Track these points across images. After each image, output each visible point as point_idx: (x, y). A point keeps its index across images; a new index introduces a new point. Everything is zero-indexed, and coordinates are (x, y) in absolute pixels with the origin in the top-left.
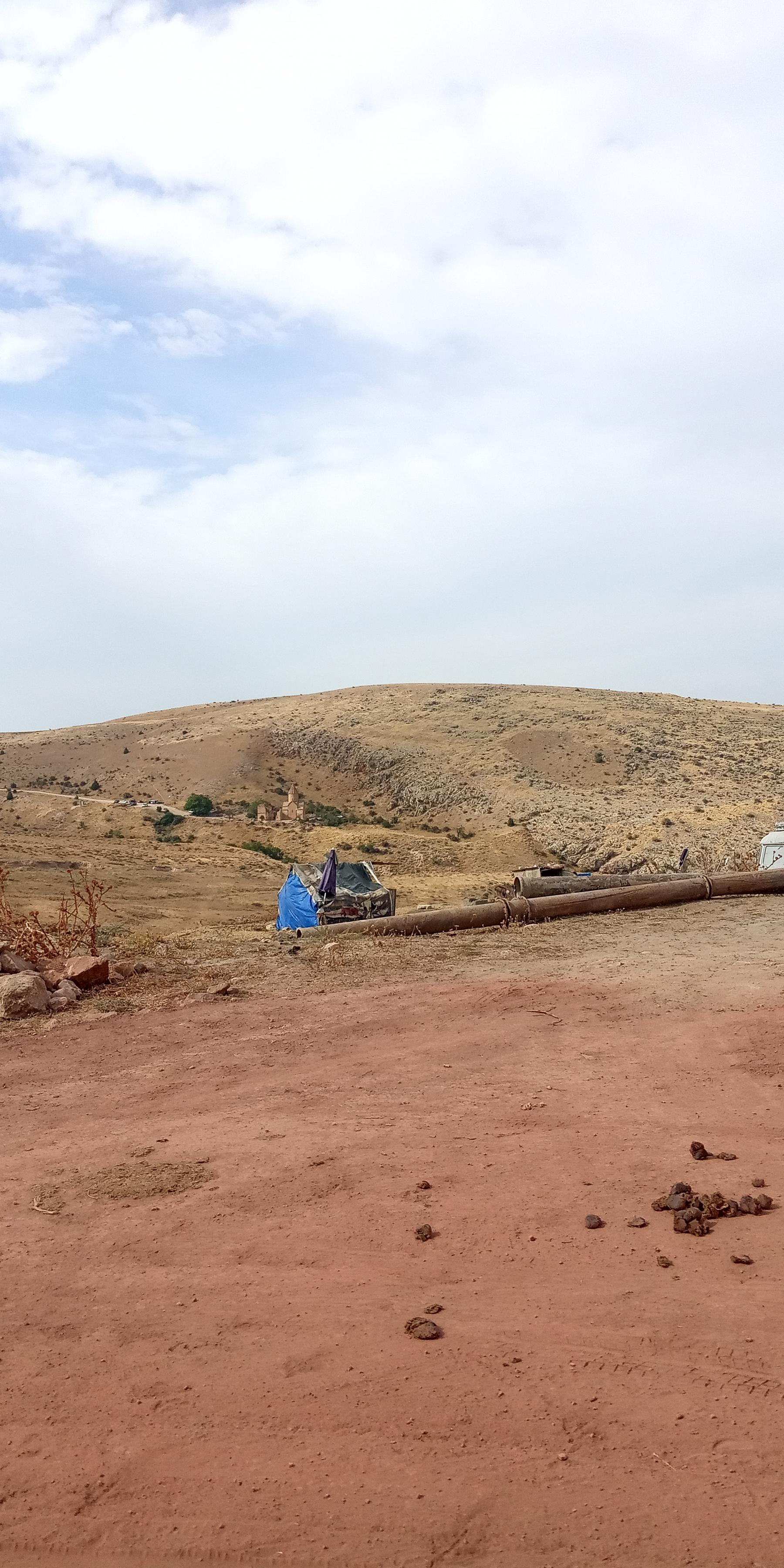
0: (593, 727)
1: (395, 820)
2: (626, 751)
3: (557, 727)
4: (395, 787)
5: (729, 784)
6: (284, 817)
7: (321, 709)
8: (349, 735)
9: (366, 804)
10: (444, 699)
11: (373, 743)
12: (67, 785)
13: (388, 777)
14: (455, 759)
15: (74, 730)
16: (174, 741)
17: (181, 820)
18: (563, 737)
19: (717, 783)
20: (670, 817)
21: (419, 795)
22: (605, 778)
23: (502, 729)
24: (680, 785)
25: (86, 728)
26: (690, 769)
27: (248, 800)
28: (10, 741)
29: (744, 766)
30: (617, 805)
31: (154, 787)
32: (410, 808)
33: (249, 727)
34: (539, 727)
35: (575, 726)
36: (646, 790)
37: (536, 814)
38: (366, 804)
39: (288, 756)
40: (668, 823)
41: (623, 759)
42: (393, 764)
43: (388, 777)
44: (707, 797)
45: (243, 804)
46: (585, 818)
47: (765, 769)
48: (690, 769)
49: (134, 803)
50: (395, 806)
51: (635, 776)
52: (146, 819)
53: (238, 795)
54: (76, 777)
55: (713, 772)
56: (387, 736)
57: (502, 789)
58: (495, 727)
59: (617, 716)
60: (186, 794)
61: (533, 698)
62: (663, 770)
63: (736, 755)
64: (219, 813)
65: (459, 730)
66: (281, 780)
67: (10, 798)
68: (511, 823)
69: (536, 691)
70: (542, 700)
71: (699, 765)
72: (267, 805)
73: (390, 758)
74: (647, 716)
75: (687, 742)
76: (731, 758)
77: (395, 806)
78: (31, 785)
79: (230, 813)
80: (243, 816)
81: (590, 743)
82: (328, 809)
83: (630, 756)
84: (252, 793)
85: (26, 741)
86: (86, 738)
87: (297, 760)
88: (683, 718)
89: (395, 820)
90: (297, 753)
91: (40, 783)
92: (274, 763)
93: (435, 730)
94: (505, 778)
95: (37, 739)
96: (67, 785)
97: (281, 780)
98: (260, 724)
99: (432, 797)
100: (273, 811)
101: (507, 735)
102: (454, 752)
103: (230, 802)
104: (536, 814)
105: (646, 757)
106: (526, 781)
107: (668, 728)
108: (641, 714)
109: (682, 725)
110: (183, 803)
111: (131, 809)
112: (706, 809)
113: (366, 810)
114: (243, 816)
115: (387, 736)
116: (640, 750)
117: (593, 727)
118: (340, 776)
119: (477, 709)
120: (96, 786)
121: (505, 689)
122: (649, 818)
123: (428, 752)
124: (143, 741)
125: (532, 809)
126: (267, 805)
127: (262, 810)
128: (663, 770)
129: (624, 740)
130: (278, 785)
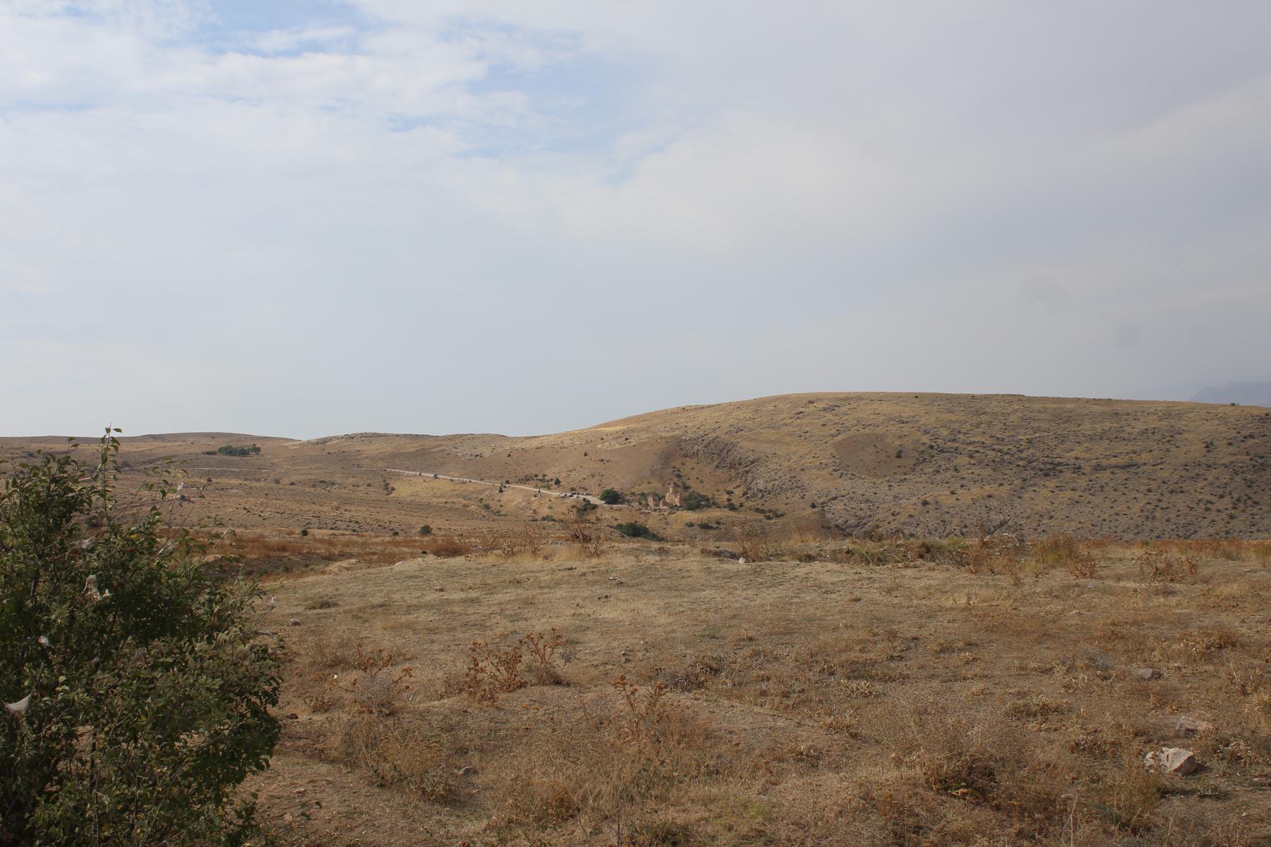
1: (741, 505)
3: (879, 431)
4: (750, 479)
11: (745, 448)
24: (948, 475)
35: (894, 429)
36: (924, 478)
41: (916, 454)
42: (752, 463)
44: (964, 482)
51: (918, 469)
56: (756, 440)
58: (834, 431)
73: (751, 459)
81: (897, 443)
89: (741, 505)
93: (791, 435)
101: (839, 438)
112: (960, 491)
115: (756, 440)
116: (931, 447)
117: (906, 429)
119: (829, 416)
129: (925, 439)
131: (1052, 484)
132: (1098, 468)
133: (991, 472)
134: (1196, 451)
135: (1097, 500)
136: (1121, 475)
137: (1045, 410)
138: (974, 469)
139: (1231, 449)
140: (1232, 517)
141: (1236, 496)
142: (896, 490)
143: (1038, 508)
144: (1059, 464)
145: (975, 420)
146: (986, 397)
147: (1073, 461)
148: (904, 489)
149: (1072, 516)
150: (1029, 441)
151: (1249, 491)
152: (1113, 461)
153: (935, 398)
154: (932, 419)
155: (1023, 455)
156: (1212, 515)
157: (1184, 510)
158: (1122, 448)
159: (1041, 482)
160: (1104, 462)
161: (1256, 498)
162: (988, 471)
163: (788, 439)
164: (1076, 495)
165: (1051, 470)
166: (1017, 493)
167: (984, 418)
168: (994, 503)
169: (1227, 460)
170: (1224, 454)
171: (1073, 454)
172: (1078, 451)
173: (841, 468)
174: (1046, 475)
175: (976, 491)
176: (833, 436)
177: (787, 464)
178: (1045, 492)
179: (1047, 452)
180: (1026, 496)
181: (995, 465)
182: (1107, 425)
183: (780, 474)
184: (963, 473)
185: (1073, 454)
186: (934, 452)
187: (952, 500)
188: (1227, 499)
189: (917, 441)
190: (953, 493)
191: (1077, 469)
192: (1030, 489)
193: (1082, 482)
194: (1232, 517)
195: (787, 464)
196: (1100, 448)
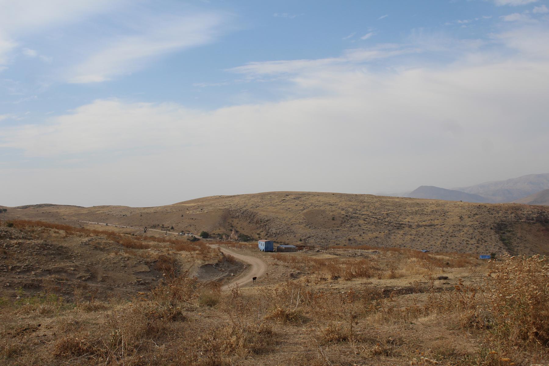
0: (334, 208)
2: (343, 216)
3: (321, 208)
5: (373, 227)
6: (231, 239)
7: (247, 201)
8: (255, 211)
9: (258, 234)
10: (288, 198)
11: (262, 214)
12: (163, 227)
13: (266, 225)
14: (287, 219)
15: (165, 207)
16: (198, 213)
17: (198, 240)
18: (324, 211)
19: (369, 227)
20: (351, 238)
21: (274, 231)
22: (334, 225)
23: (304, 209)
24: (357, 228)
25: (169, 206)
26: (361, 222)
27: (220, 233)
28: (143, 211)
29: (379, 221)
30: (335, 234)
31: (191, 229)
32: (271, 235)
33: (223, 208)
34: (316, 208)
35: (328, 208)
36: (346, 229)
37: (309, 237)
38: (258, 234)
39: (235, 218)
40: (350, 240)
41: (341, 219)
42: (267, 221)
43: (266, 225)
44: (364, 231)
45: (219, 234)
46: (324, 239)
47: (386, 222)
48: (361, 222)
49: (184, 234)
50: (267, 235)
51: (343, 225)
52: (188, 239)
53: (217, 231)
54: (166, 225)
55: (369, 223)
56: (267, 211)
57: (301, 229)
58: (302, 208)
59: (343, 204)
60: (201, 231)
61: (317, 197)
62: (353, 223)
63: (378, 217)
64: (211, 237)
65: (290, 209)
66: (232, 226)
67: (145, 232)
68: (301, 240)
69: (319, 194)
70: (320, 198)
71: (365, 220)
72: (226, 234)
73: (266, 219)
74: (353, 204)
75: (363, 213)
76: (376, 218)
77: (267, 235)
78: (151, 227)
79: (214, 238)
80: (218, 238)
81: (331, 214)
82: (246, 236)
83: (343, 218)
84: (222, 230)
85: (149, 211)
86: (169, 210)
87: (238, 219)
88: (365, 204)
90: (238, 217)
91: (154, 227)
92: (230, 221)
94: (302, 226)
95: (152, 211)
96: (163, 227)
97: (232, 226)
98: (226, 207)
99: (278, 232)
100: (228, 236)
101: (305, 211)
102: (287, 217)
103: (214, 234)
104: (309, 237)
105: (348, 218)
106: (308, 227)
107: (359, 208)
108: (351, 203)
109: (364, 207)
110: (200, 234)
111: (184, 236)
112: (363, 235)
113: (258, 236)
114: (218, 238)
115: (267, 211)
116: (347, 216)
118: (251, 225)
120: (172, 228)
121: (309, 194)
122: (345, 238)
123: (279, 217)
124: (188, 212)
125: (309, 236)
126: (226, 234)
127: (224, 237)
128: (353, 223)
129: (343, 212)
130: (231, 228)
131: (401, 232)
132: (418, 226)
133: (374, 227)
134: (456, 220)
135: (422, 239)
136: (429, 229)
137: (389, 202)
138: (367, 226)
139: (470, 219)
140: (478, 247)
141: (477, 238)
142: (335, 234)
143: (398, 243)
144: (402, 224)
145: (362, 205)
146: (362, 195)
147: (407, 223)
148: (339, 233)
149: (413, 246)
150: (387, 214)
151: (481, 236)
152: (424, 223)
153: (341, 195)
154: (344, 204)
155: (386, 220)
156: (470, 246)
157: (459, 244)
158: (426, 218)
159: (397, 232)
160: (421, 224)
161: (485, 239)
162: (373, 227)
163: (282, 211)
164: (413, 237)
165: (400, 226)
166: (388, 236)
167: (365, 204)
168: (379, 240)
169: (470, 224)
170: (468, 221)
171: (407, 220)
172: (408, 219)
173: (309, 224)
174: (398, 229)
175: (370, 234)
176: (302, 210)
177: (284, 222)
178: (399, 235)
179: (396, 219)
180: (392, 237)
181: (376, 224)
182: (417, 209)
183: (282, 226)
184: (363, 227)
185: (407, 220)
186: (348, 218)
187: (360, 239)
188: (474, 240)
189: (340, 213)
190: (360, 235)
191: (410, 226)
192: (393, 234)
193: (414, 232)
194: (478, 247)
195: (284, 222)
196: (417, 218)
